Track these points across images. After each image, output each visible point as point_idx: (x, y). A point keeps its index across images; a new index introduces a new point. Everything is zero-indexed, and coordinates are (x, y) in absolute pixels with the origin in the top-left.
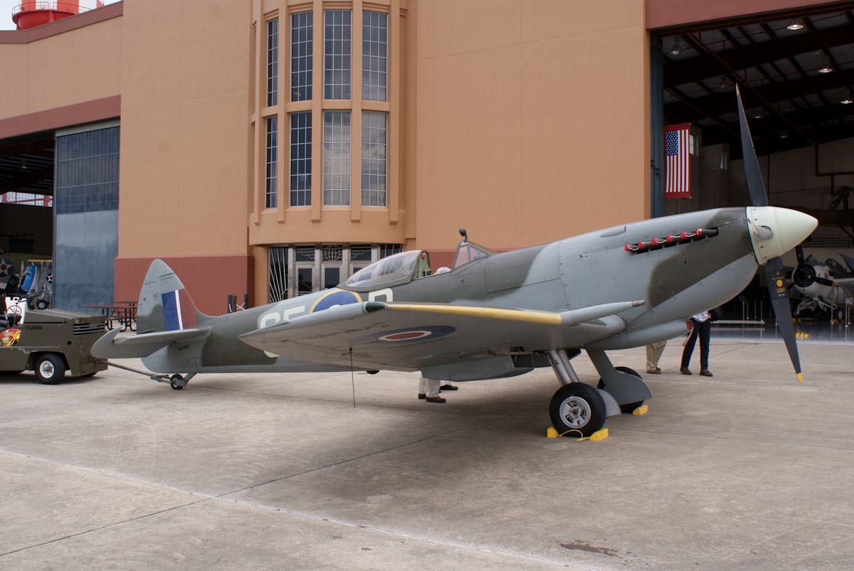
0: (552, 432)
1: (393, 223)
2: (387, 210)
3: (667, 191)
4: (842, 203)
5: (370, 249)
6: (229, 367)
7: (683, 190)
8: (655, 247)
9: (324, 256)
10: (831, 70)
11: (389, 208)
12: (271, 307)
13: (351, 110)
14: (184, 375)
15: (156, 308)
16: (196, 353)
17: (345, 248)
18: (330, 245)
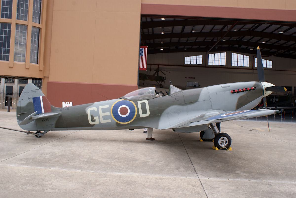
0: (217, 149)
1: (41, 71)
2: (39, 65)
3: (140, 68)
4: (157, 73)
5: (1, 78)
6: (68, 128)
7: (143, 68)
8: (238, 92)
9: (6, 81)
10: (164, 33)
11: (40, 65)
12: (92, 105)
13: (11, 23)
14: (42, 132)
15: (29, 104)
16: (53, 123)
17: (16, 78)
18: (9, 77)
